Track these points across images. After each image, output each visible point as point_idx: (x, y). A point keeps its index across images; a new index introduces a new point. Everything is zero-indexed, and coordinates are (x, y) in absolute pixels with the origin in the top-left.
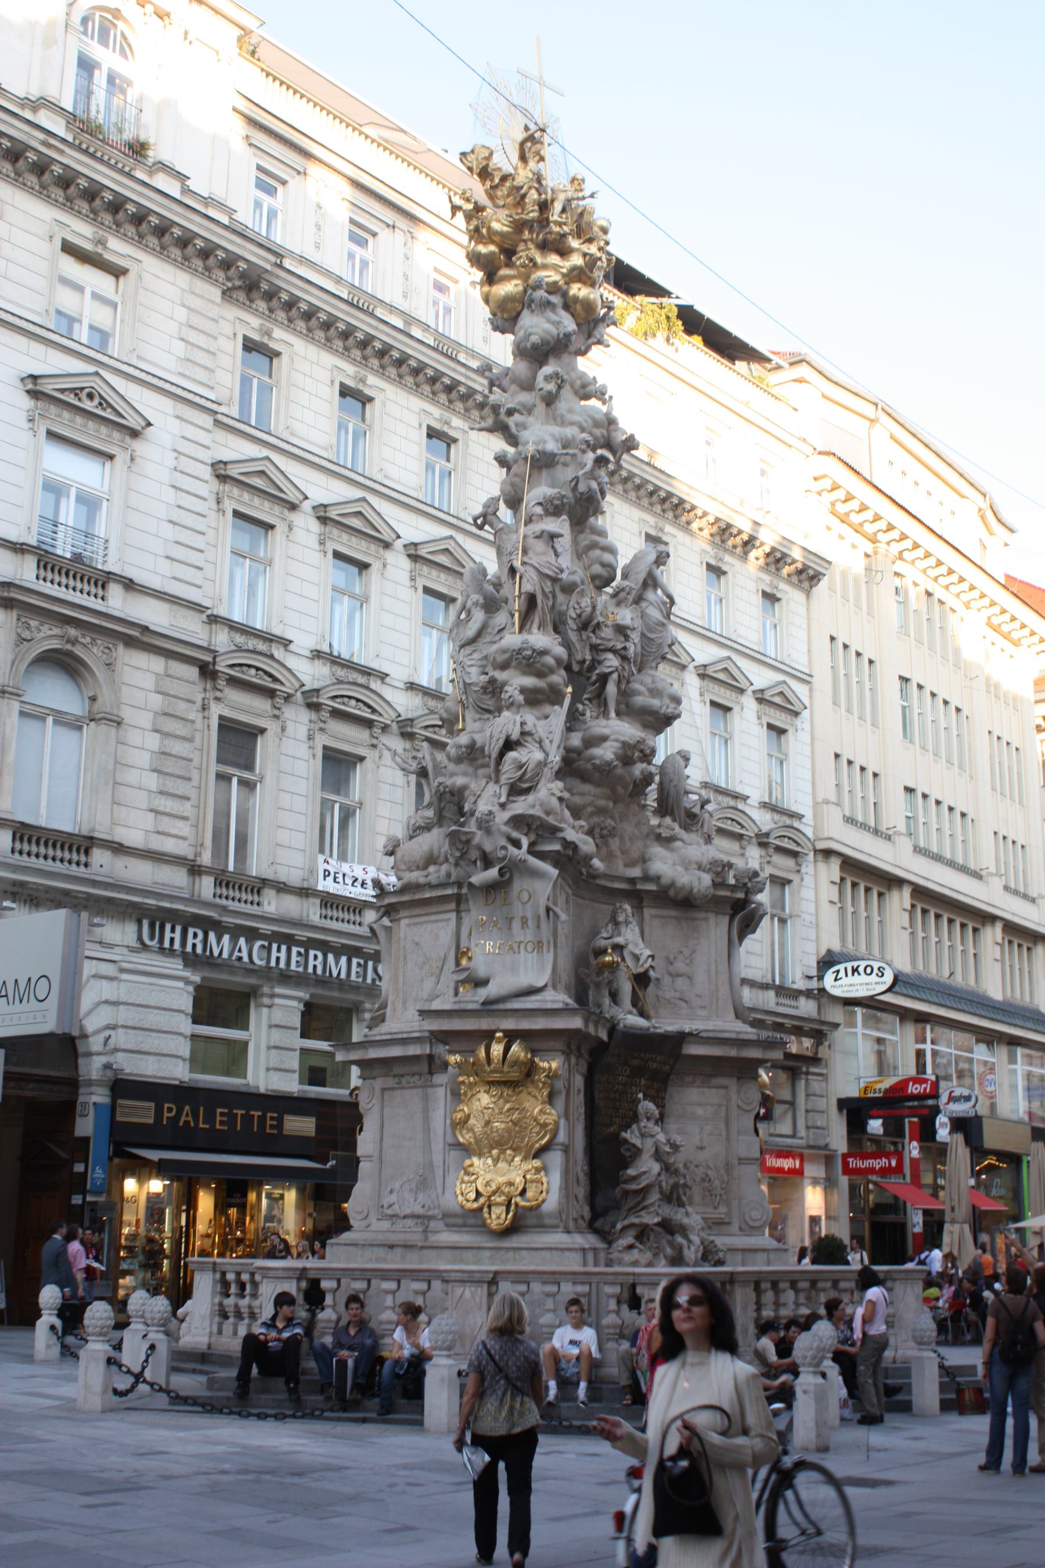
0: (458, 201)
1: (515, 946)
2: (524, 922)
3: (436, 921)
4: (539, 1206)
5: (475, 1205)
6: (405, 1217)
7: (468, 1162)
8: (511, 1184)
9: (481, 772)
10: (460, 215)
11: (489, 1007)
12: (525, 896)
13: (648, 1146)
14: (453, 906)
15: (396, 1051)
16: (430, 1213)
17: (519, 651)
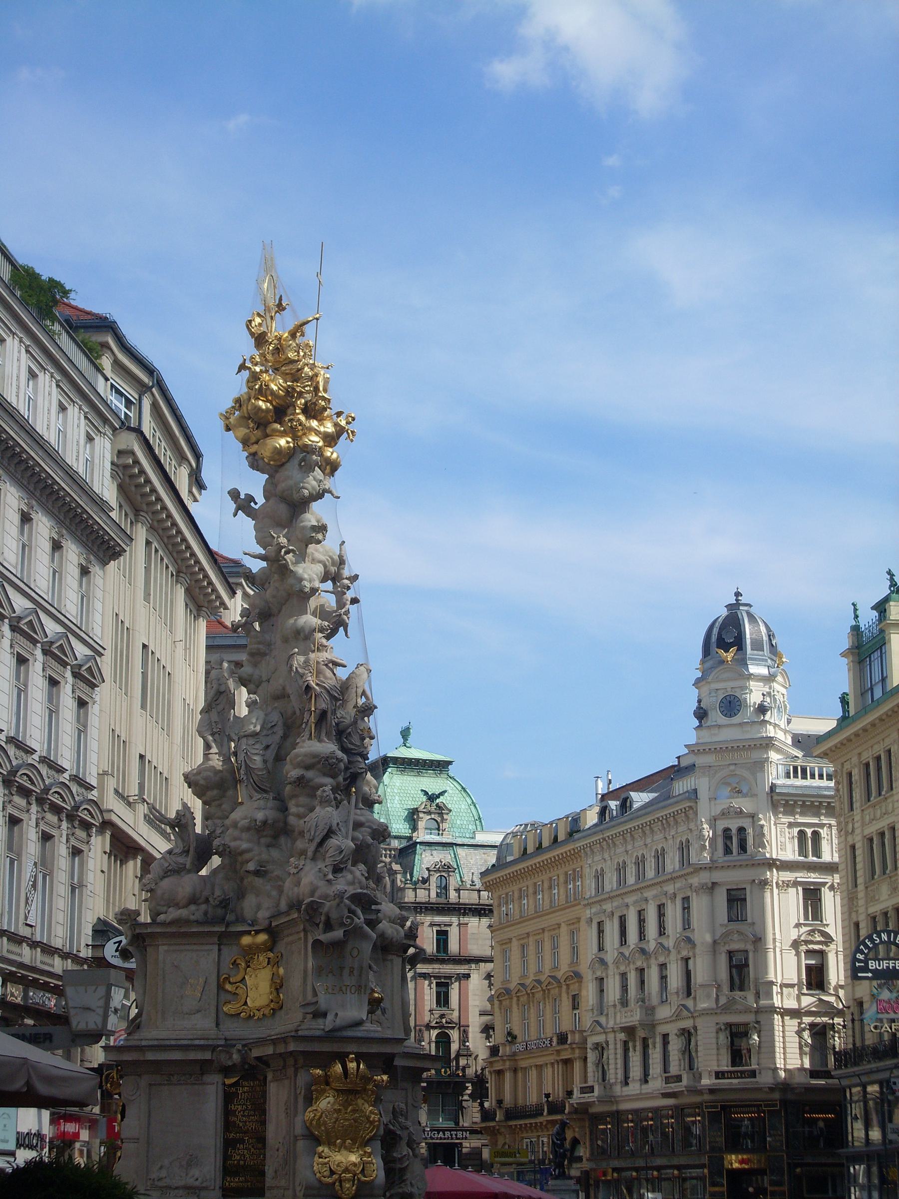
0: (248, 364)
1: (344, 988)
2: (351, 972)
3: (197, 950)
4: (373, 1180)
5: (329, 1180)
6: (177, 1188)
7: (320, 1149)
8: (355, 1165)
9: (263, 840)
10: (246, 374)
11: (331, 1035)
12: (355, 953)
13: (404, 1134)
14: (216, 939)
15: (177, 1056)
16: (204, 1185)
17: (327, 759)
